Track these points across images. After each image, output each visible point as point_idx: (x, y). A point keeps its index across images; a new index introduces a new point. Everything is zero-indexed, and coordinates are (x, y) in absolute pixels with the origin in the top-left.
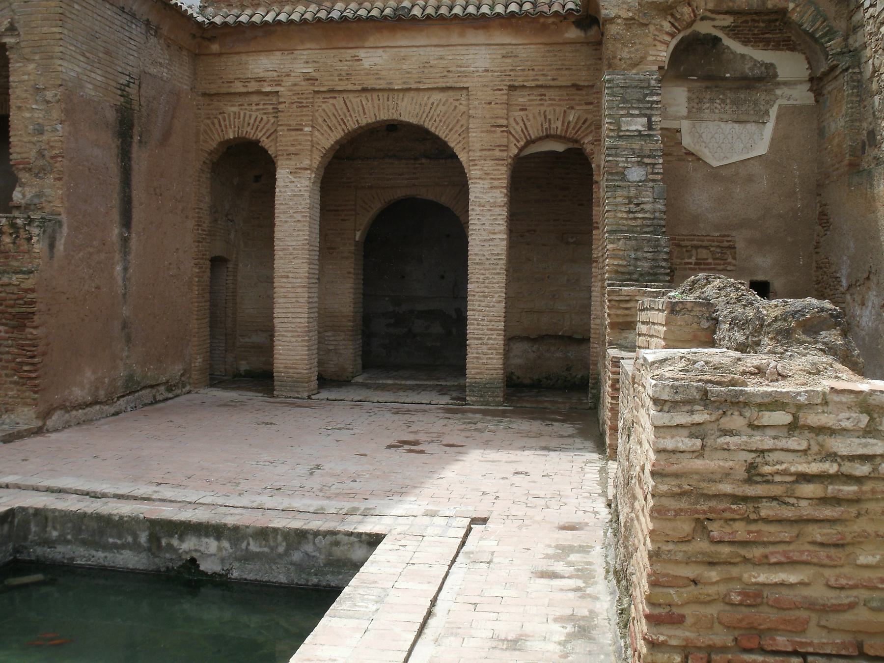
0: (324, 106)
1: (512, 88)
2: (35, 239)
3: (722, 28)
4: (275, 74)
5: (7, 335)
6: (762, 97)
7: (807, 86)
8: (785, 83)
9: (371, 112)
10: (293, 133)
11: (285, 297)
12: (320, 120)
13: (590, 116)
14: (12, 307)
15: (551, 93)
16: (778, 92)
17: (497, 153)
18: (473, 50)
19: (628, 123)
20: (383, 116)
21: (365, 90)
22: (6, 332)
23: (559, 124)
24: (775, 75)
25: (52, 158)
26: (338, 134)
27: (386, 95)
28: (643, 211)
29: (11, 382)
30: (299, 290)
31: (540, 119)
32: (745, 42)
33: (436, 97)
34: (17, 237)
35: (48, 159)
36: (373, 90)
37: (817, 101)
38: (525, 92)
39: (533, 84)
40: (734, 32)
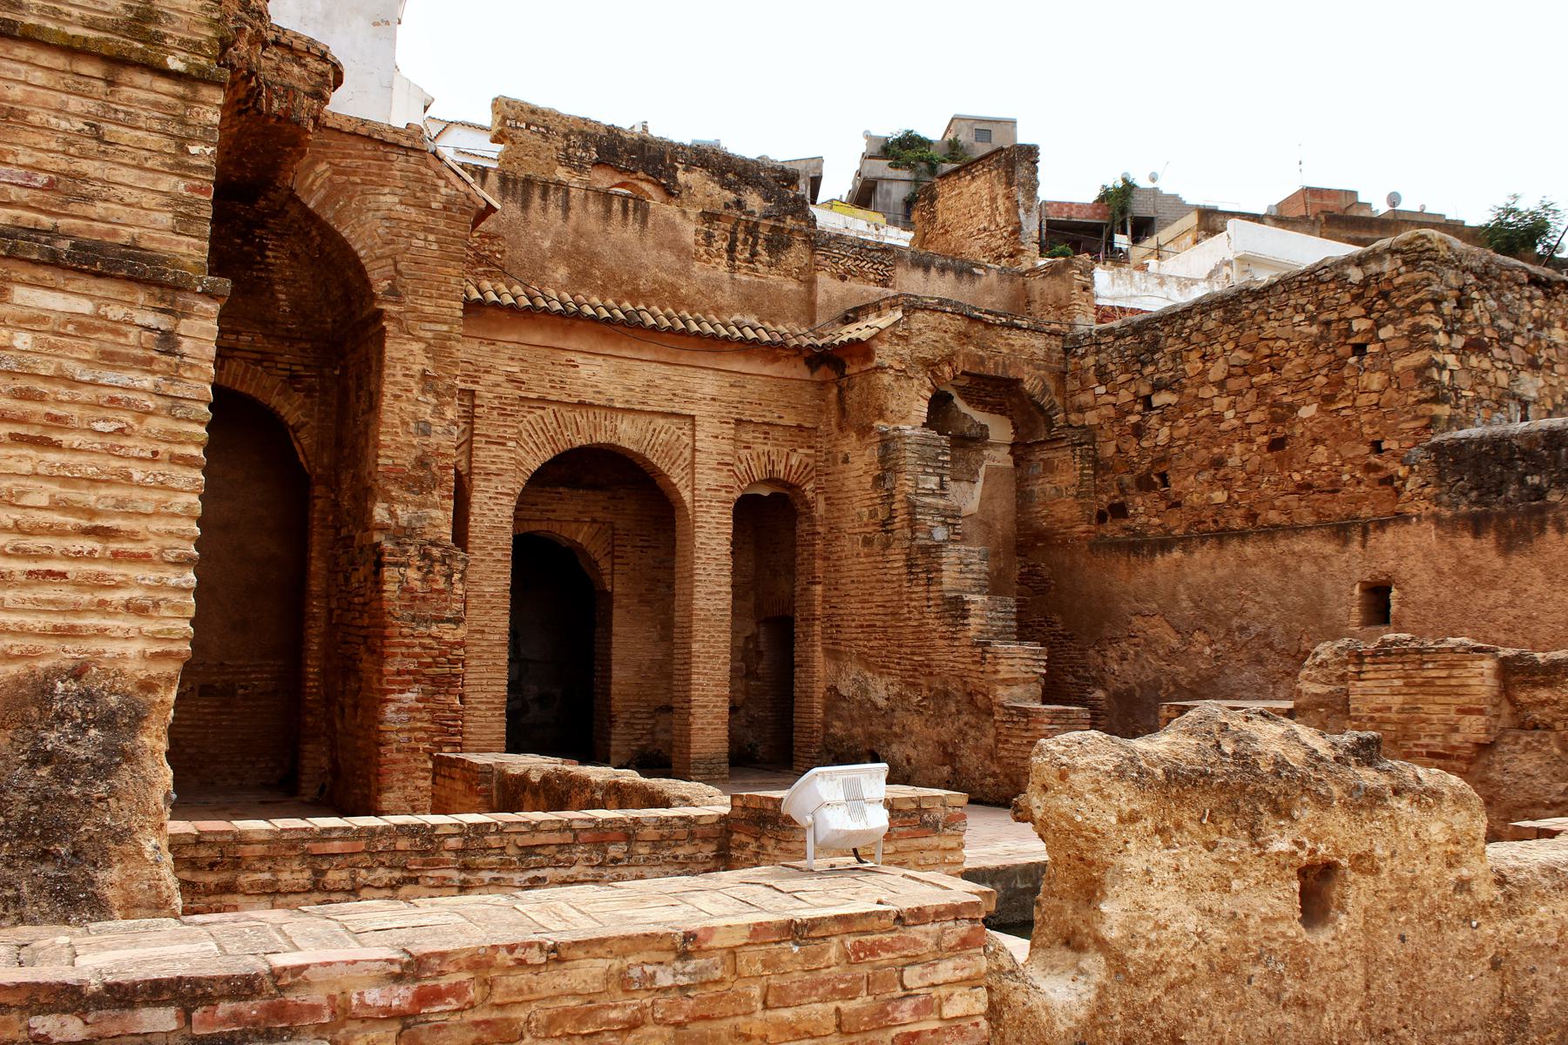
0: (530, 417)
1: (739, 422)
2: (457, 576)
3: (957, 387)
4: (471, 368)
5: (421, 705)
6: (973, 456)
7: (1008, 449)
8: (992, 445)
9: (583, 432)
10: (494, 447)
11: (480, 658)
12: (525, 435)
13: (811, 461)
14: (429, 665)
15: (776, 433)
16: (985, 453)
17: (723, 494)
18: (700, 374)
19: (925, 481)
20: (601, 438)
21: (581, 404)
22: (418, 700)
23: (782, 467)
24: (987, 437)
25: (440, 468)
26: (547, 454)
27: (603, 412)
28: (972, 571)
29: (423, 770)
30: (497, 649)
31: (764, 459)
32: (969, 403)
33: (660, 422)
34: (430, 572)
35: (435, 469)
36: (591, 405)
37: (1016, 465)
38: (751, 427)
39: (760, 420)
40: (966, 394)
